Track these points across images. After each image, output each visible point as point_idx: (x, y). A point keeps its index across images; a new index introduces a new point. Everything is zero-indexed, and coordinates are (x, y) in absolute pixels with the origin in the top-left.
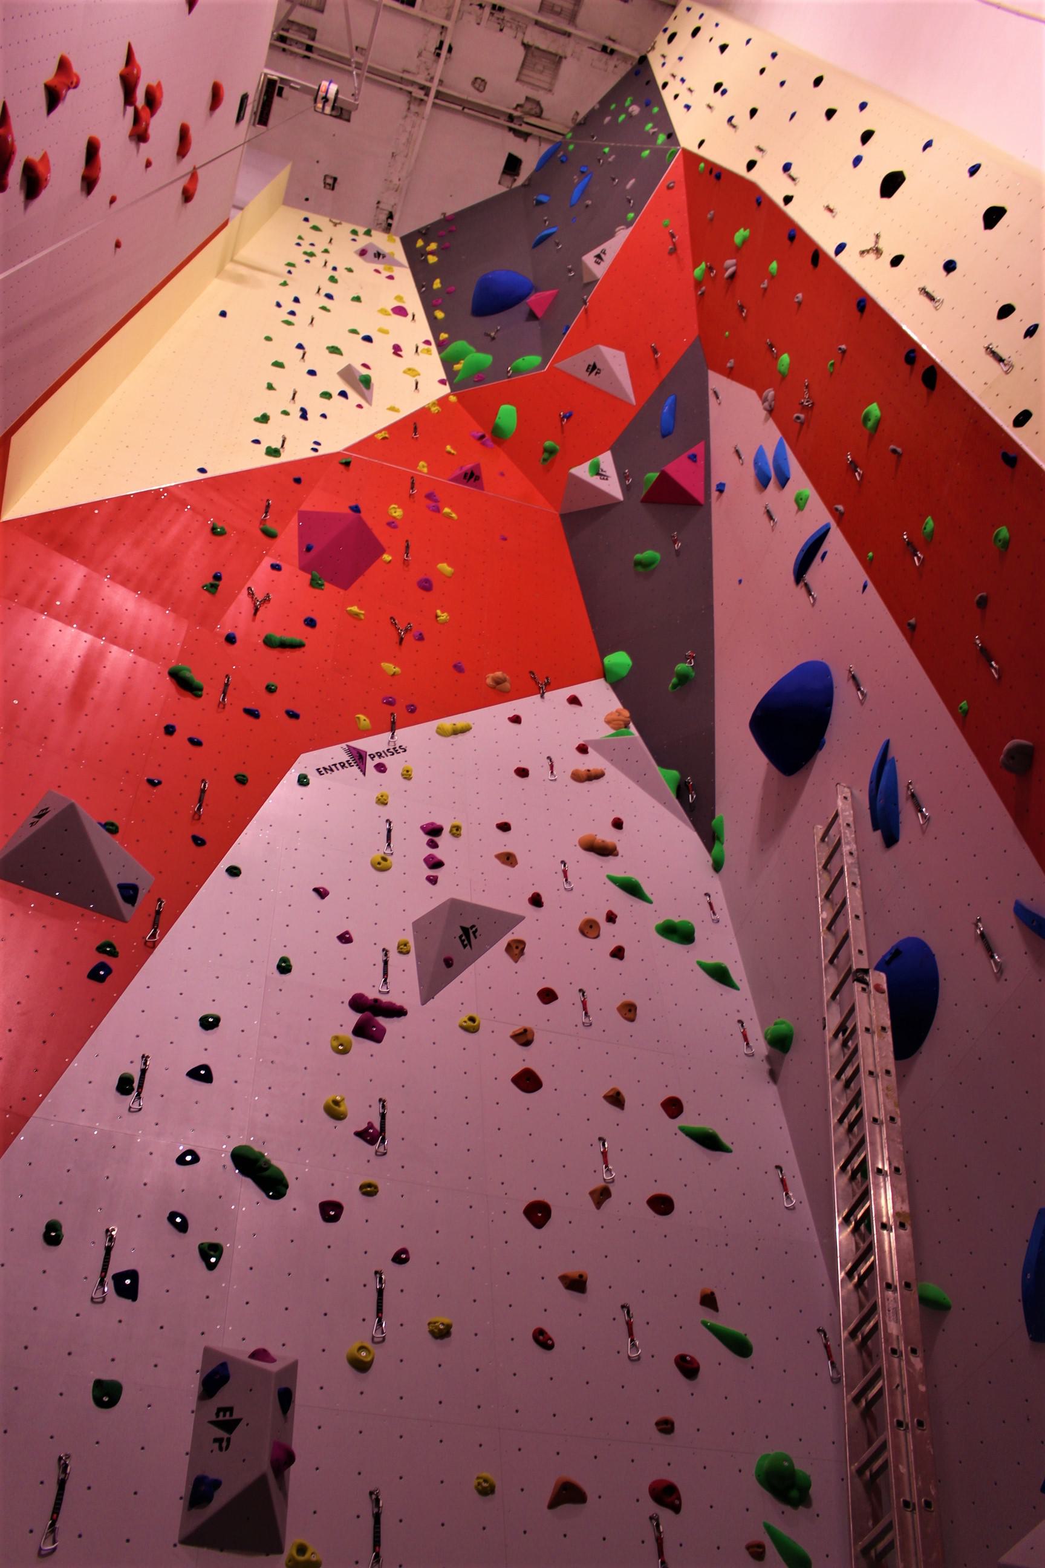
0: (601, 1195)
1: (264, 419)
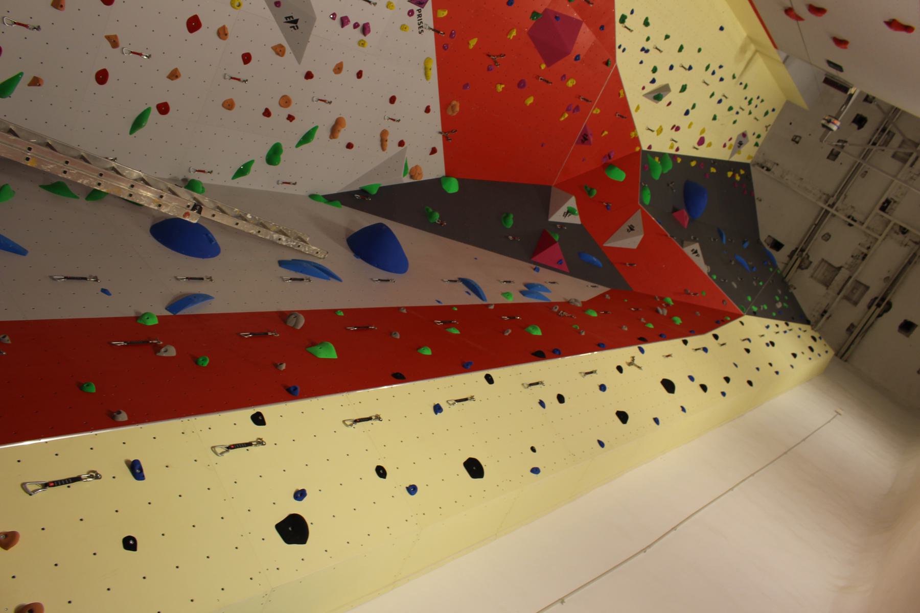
0: (114, 42)
1: (646, 23)
